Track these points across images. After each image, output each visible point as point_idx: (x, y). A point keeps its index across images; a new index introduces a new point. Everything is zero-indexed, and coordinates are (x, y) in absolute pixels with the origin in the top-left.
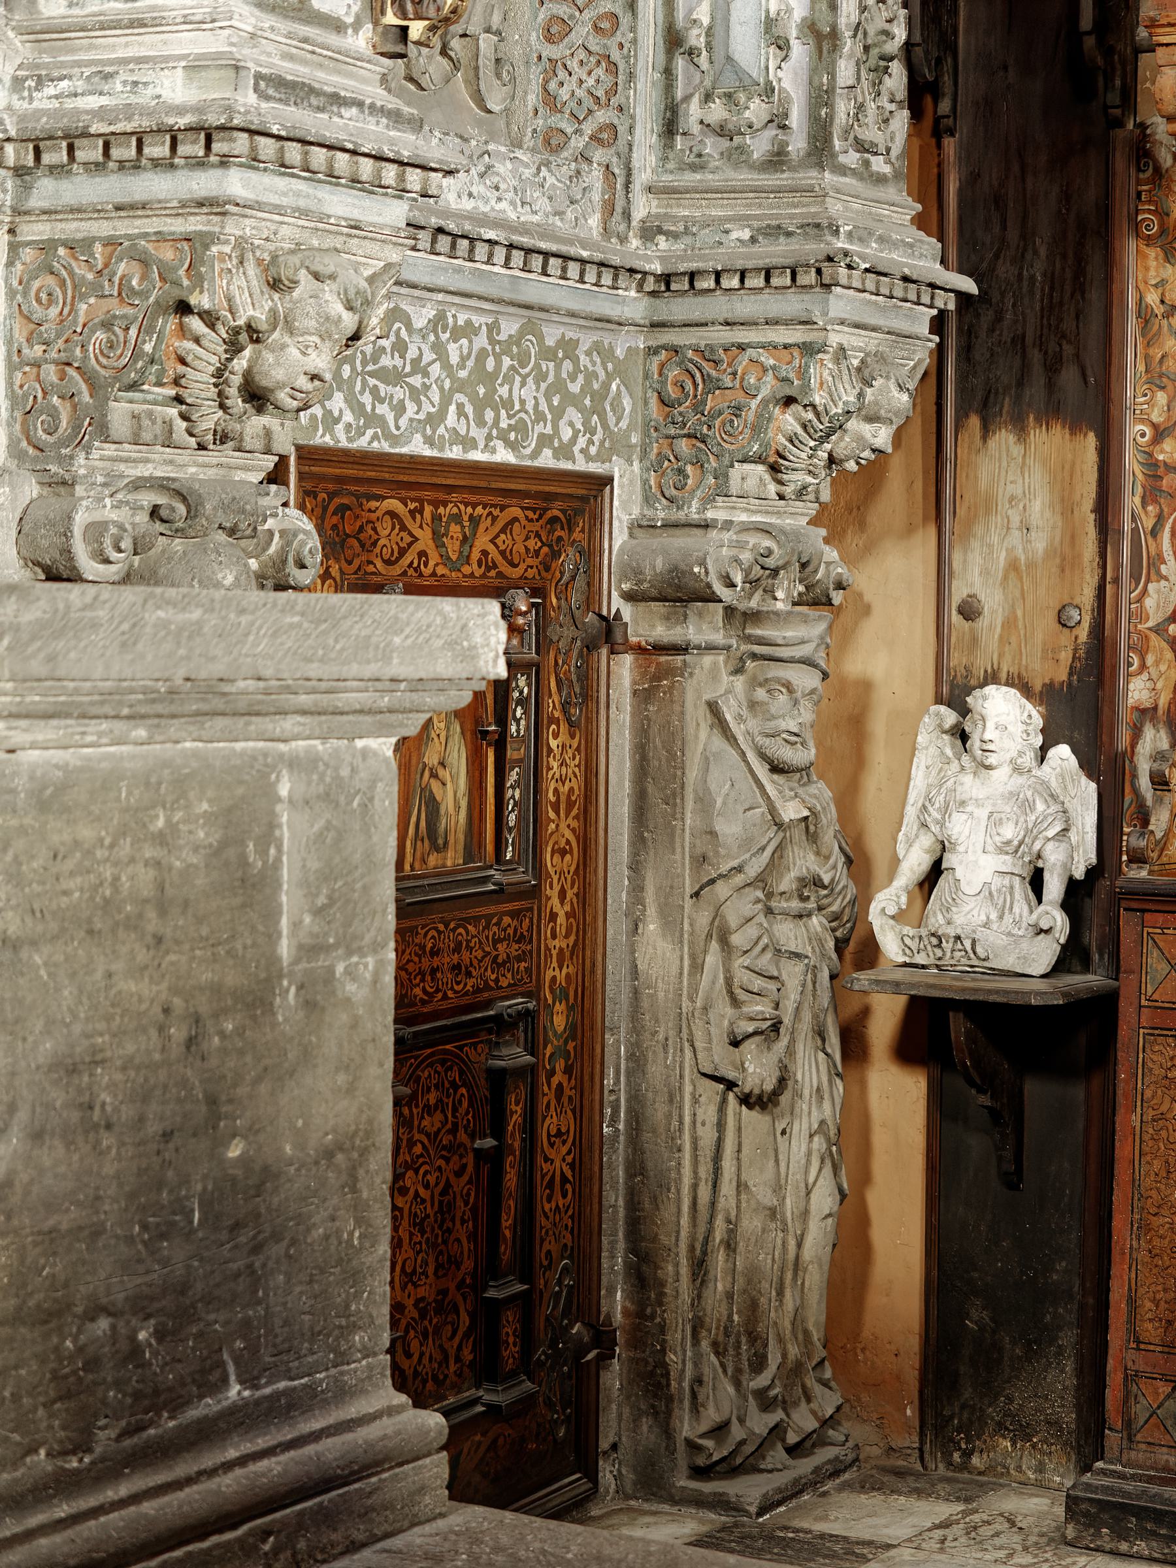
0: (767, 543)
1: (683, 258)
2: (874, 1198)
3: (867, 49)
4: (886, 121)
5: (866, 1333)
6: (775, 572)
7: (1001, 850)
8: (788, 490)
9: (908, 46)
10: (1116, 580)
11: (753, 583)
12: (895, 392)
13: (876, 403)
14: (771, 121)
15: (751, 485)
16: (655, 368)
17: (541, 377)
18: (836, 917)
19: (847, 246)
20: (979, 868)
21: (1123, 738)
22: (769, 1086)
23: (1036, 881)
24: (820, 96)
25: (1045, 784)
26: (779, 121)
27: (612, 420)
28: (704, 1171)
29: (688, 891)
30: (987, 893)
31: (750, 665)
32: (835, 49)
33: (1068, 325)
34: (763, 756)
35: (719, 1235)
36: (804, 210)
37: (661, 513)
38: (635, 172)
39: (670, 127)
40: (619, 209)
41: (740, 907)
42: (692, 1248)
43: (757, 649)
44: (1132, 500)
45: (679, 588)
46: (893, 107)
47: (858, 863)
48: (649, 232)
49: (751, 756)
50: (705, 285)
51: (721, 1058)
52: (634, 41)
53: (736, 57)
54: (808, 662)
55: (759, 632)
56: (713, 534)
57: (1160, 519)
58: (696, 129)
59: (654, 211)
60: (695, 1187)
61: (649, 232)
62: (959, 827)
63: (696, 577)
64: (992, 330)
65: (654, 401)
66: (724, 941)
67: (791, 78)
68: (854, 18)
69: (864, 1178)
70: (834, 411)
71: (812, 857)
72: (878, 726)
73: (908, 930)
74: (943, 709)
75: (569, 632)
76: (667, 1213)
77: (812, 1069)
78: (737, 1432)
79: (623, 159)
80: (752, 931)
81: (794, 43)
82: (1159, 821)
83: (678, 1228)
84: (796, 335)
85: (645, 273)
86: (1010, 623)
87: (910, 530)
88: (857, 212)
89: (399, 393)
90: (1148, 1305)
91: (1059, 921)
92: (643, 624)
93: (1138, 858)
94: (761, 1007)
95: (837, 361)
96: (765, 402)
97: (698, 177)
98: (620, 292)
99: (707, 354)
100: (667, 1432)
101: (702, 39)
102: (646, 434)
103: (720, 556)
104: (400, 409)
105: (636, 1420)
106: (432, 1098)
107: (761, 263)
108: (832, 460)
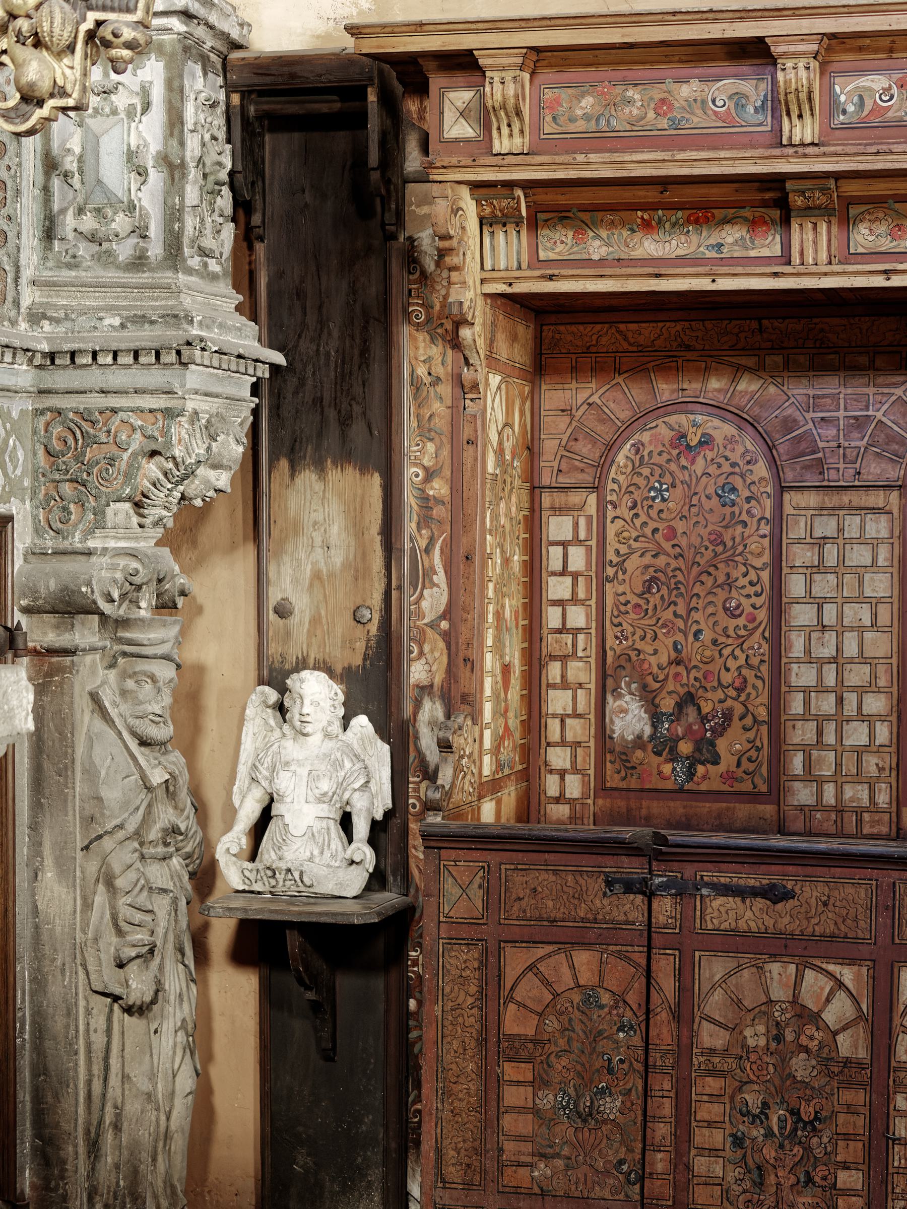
0: (135, 565)
1: (66, 339)
2: (216, 1073)
3: (205, 176)
4: (219, 232)
5: (211, 1178)
6: (139, 588)
7: (320, 800)
8: (147, 521)
9: (231, 174)
10: (400, 588)
11: (123, 596)
13: (220, 454)
14: (133, 232)
15: (121, 518)
16: (41, 426)
18: (188, 856)
19: (203, 334)
21: (408, 709)
22: (148, 998)
23: (346, 822)
24: (173, 213)
25: (349, 746)
26: (141, 232)
27: (10, 468)
28: (97, 1069)
29: (79, 845)
31: (121, 661)
32: (184, 176)
33: (357, 390)
34: (134, 734)
35: (108, 1119)
36: (163, 303)
37: (50, 542)
38: (22, 269)
39: (49, 234)
40: (10, 299)
41: (122, 856)
42: (87, 1132)
43: (127, 648)
44: (410, 526)
45: (69, 604)
46: (221, 220)
47: (201, 810)
48: (35, 318)
49: (126, 735)
50: (84, 361)
51: (111, 980)
52: (19, 165)
53: (105, 180)
54: (166, 658)
55: (128, 635)
56: (94, 559)
58: (71, 235)
59: (37, 300)
60: (89, 1083)
62: (284, 783)
63: (84, 595)
64: (296, 393)
65: (41, 452)
66: (110, 883)
67: (150, 197)
68: (197, 153)
69: (208, 1057)
70: (188, 461)
71: (171, 810)
72: (211, 700)
74: (266, 689)
76: (66, 1104)
77: (175, 980)
79: (13, 259)
80: (132, 875)
81: (151, 171)
82: (445, 776)
85: (35, 351)
86: (315, 621)
87: (233, 547)
88: (200, 303)
90: (452, 1153)
91: (367, 855)
92: (40, 633)
93: (430, 806)
94: (141, 936)
95: (192, 422)
96: (134, 455)
97: (74, 274)
98: (16, 366)
99: (85, 415)
101: (75, 165)
102: (35, 479)
103: (101, 577)
107: (132, 346)
108: (183, 497)
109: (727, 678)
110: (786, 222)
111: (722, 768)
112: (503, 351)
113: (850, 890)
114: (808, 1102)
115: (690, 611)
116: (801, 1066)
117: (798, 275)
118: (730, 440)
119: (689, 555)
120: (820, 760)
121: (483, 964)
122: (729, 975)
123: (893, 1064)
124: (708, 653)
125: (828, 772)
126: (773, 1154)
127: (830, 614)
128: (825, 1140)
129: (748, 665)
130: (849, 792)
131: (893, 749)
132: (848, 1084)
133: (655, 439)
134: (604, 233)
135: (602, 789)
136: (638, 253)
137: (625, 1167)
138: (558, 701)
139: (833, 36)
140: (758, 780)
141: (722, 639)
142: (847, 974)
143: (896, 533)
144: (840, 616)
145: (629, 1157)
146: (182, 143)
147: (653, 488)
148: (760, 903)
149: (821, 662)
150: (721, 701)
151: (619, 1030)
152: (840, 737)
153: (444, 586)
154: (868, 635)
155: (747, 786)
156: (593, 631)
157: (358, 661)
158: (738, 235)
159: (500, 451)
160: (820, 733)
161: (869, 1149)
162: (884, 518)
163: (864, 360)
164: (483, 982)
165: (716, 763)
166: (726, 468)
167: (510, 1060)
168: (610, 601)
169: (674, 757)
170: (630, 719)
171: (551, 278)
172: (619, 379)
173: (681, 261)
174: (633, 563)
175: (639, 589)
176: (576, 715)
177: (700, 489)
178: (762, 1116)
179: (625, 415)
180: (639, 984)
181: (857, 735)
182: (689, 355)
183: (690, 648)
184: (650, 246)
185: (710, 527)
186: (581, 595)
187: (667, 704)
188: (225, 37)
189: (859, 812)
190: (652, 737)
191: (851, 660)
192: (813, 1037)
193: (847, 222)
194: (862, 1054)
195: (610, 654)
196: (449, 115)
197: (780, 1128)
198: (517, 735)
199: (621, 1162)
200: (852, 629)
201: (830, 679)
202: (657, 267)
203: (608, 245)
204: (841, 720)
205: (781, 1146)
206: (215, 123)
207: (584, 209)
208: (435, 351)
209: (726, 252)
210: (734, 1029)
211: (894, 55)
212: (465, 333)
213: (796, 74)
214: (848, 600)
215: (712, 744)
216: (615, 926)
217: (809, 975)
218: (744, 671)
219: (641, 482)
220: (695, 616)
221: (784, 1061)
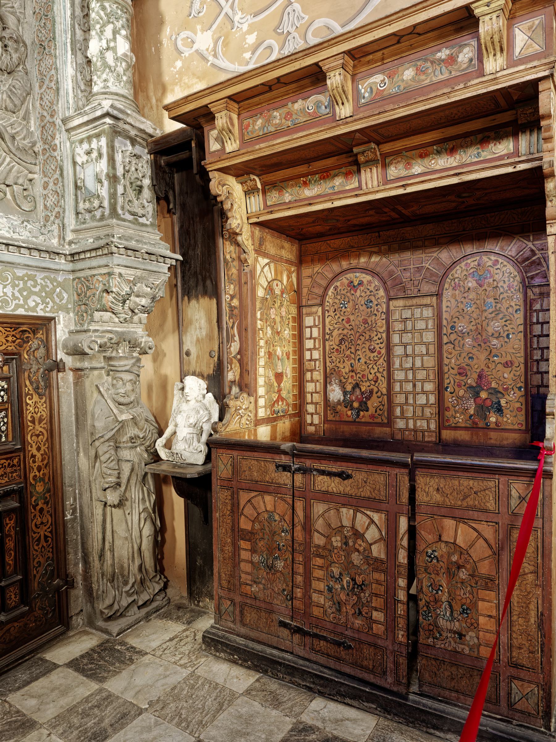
0: (111, 335)
5: (176, 562)
7: (189, 427)
12: (145, 288)
16: (75, 284)
17: (14, 286)
20: (184, 432)
21: (227, 390)
25: (204, 405)
27: (57, 300)
30: (185, 440)
34: (114, 401)
43: (112, 368)
44: (225, 318)
49: (109, 401)
53: (87, 186)
55: (112, 363)
57: (234, 323)
61: (70, 243)
64: (189, 271)
65: (75, 294)
67: (104, 192)
73: (167, 450)
77: (135, 493)
78: (116, 607)
84: (104, 270)
86: (198, 357)
100: (93, 607)
105: (86, 603)
109: (371, 377)
110: (359, 171)
111: (370, 413)
113: (376, 476)
114: (359, 575)
115: (356, 350)
116: (356, 558)
117: (366, 194)
118: (370, 282)
119: (355, 329)
120: (407, 410)
122: (325, 512)
123: (397, 563)
124: (363, 367)
125: (410, 414)
126: (345, 598)
127: (409, 349)
128: (367, 595)
129: (380, 372)
130: (419, 423)
131: (437, 405)
133: (342, 284)
134: (289, 190)
135: (326, 421)
136: (302, 197)
137: (286, 593)
138: (310, 387)
139: (350, 53)
140: (383, 418)
141: (368, 362)
143: (436, 315)
144: (414, 350)
145: (287, 588)
146: (114, 168)
147: (341, 303)
148: (337, 480)
149: (407, 370)
150: (369, 386)
151: (283, 531)
152: (415, 401)
153: (238, 341)
154: (425, 358)
155: (379, 420)
156: (322, 360)
157: (211, 372)
158: (340, 181)
159: (270, 289)
160: (407, 399)
161: (386, 602)
162: (430, 309)
163: (420, 243)
164: (233, 505)
165: (367, 411)
166: (368, 293)
167: (243, 539)
168: (327, 348)
169: (352, 408)
170: (336, 394)
171: (271, 212)
172: (328, 262)
173: (319, 196)
174: (335, 333)
175: (337, 343)
176: (316, 392)
177: (359, 302)
178: (339, 579)
179: (330, 276)
180: (290, 512)
181: (422, 400)
182: (353, 250)
183: (358, 367)
184: (308, 193)
185: (363, 317)
186: (317, 346)
187: (349, 388)
189: (423, 432)
190: (344, 401)
191: (418, 369)
193: (385, 166)
195: (328, 368)
196: (212, 141)
197: (348, 586)
198: (291, 401)
199: (284, 590)
200: (418, 356)
201: (410, 377)
203: (292, 195)
204: (415, 394)
205: (348, 595)
206: (140, 165)
209: (336, 189)
210: (328, 538)
211: (385, 62)
212: (239, 238)
213: (335, 79)
214: (416, 344)
215: (366, 404)
216: (279, 486)
218: (377, 374)
219: (337, 301)
220: (358, 353)
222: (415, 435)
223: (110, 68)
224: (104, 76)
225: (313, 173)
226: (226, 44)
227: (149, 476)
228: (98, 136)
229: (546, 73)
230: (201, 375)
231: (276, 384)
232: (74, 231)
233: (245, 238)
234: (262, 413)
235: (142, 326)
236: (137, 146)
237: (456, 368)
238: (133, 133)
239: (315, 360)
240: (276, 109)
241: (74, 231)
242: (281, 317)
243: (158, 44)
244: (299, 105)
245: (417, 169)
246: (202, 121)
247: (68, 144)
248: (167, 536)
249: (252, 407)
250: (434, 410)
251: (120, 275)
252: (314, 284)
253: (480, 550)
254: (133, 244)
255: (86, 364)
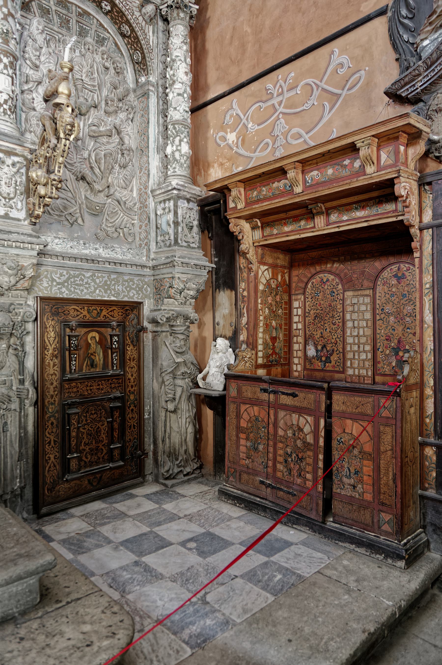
17: (123, 285)
22: (173, 410)
27: (144, 292)
34: (174, 351)
44: (239, 303)
61: (153, 260)
67: (171, 231)
75: (132, 329)
77: (184, 406)
83: (160, 434)
84: (170, 276)
86: (224, 325)
89: (82, 288)
104: (83, 290)
106: (93, 412)
110: (314, 218)
111: (332, 364)
112: (270, 261)
115: (325, 323)
118: (333, 280)
120: (354, 363)
121: (237, 408)
122: (285, 416)
125: (356, 366)
132: (309, 450)
133: (316, 281)
135: (305, 369)
142: (309, 419)
144: (359, 324)
146: (177, 218)
148: (291, 397)
149: (354, 337)
152: (359, 357)
159: (268, 284)
160: (354, 356)
162: (369, 298)
163: (363, 256)
164: (237, 412)
169: (321, 361)
170: (311, 352)
171: (266, 240)
174: (312, 312)
179: (309, 276)
181: (363, 356)
183: (326, 334)
187: (319, 348)
188: (195, 194)
189: (364, 377)
192: (301, 435)
193: (328, 215)
194: (312, 442)
196: (230, 202)
201: (356, 341)
202: (287, 234)
204: (359, 352)
207: (272, 222)
208: (244, 261)
209: (302, 228)
212: (248, 255)
213: (291, 174)
217: (301, 418)
221: (295, 442)
222: (359, 379)
223: (177, 161)
224: (174, 166)
225: (289, 218)
226: (243, 140)
227: (193, 396)
228: (169, 200)
229: (396, 175)
230: (225, 337)
231: (271, 344)
232: (154, 252)
233: (251, 255)
234: (260, 361)
235: (191, 307)
236: (191, 203)
237: (384, 335)
238: (188, 196)
239: (299, 330)
240: (264, 186)
241: (154, 252)
242: (276, 302)
243: (206, 139)
244: (276, 185)
245: (345, 218)
246: (226, 191)
247: (153, 204)
248: (203, 436)
249: (253, 357)
250: (371, 363)
251: (179, 278)
252: (300, 281)
253: (364, 438)
254: (186, 260)
255: (159, 329)
